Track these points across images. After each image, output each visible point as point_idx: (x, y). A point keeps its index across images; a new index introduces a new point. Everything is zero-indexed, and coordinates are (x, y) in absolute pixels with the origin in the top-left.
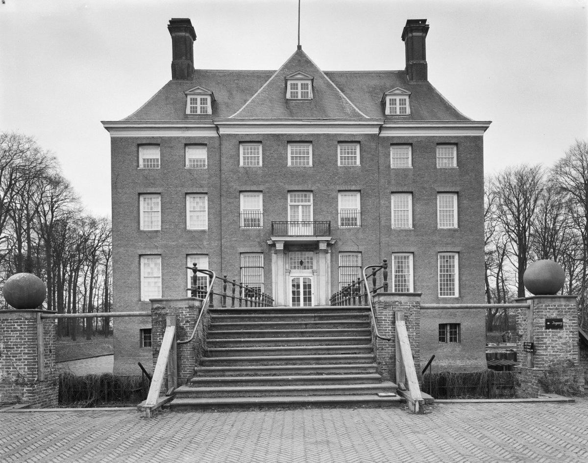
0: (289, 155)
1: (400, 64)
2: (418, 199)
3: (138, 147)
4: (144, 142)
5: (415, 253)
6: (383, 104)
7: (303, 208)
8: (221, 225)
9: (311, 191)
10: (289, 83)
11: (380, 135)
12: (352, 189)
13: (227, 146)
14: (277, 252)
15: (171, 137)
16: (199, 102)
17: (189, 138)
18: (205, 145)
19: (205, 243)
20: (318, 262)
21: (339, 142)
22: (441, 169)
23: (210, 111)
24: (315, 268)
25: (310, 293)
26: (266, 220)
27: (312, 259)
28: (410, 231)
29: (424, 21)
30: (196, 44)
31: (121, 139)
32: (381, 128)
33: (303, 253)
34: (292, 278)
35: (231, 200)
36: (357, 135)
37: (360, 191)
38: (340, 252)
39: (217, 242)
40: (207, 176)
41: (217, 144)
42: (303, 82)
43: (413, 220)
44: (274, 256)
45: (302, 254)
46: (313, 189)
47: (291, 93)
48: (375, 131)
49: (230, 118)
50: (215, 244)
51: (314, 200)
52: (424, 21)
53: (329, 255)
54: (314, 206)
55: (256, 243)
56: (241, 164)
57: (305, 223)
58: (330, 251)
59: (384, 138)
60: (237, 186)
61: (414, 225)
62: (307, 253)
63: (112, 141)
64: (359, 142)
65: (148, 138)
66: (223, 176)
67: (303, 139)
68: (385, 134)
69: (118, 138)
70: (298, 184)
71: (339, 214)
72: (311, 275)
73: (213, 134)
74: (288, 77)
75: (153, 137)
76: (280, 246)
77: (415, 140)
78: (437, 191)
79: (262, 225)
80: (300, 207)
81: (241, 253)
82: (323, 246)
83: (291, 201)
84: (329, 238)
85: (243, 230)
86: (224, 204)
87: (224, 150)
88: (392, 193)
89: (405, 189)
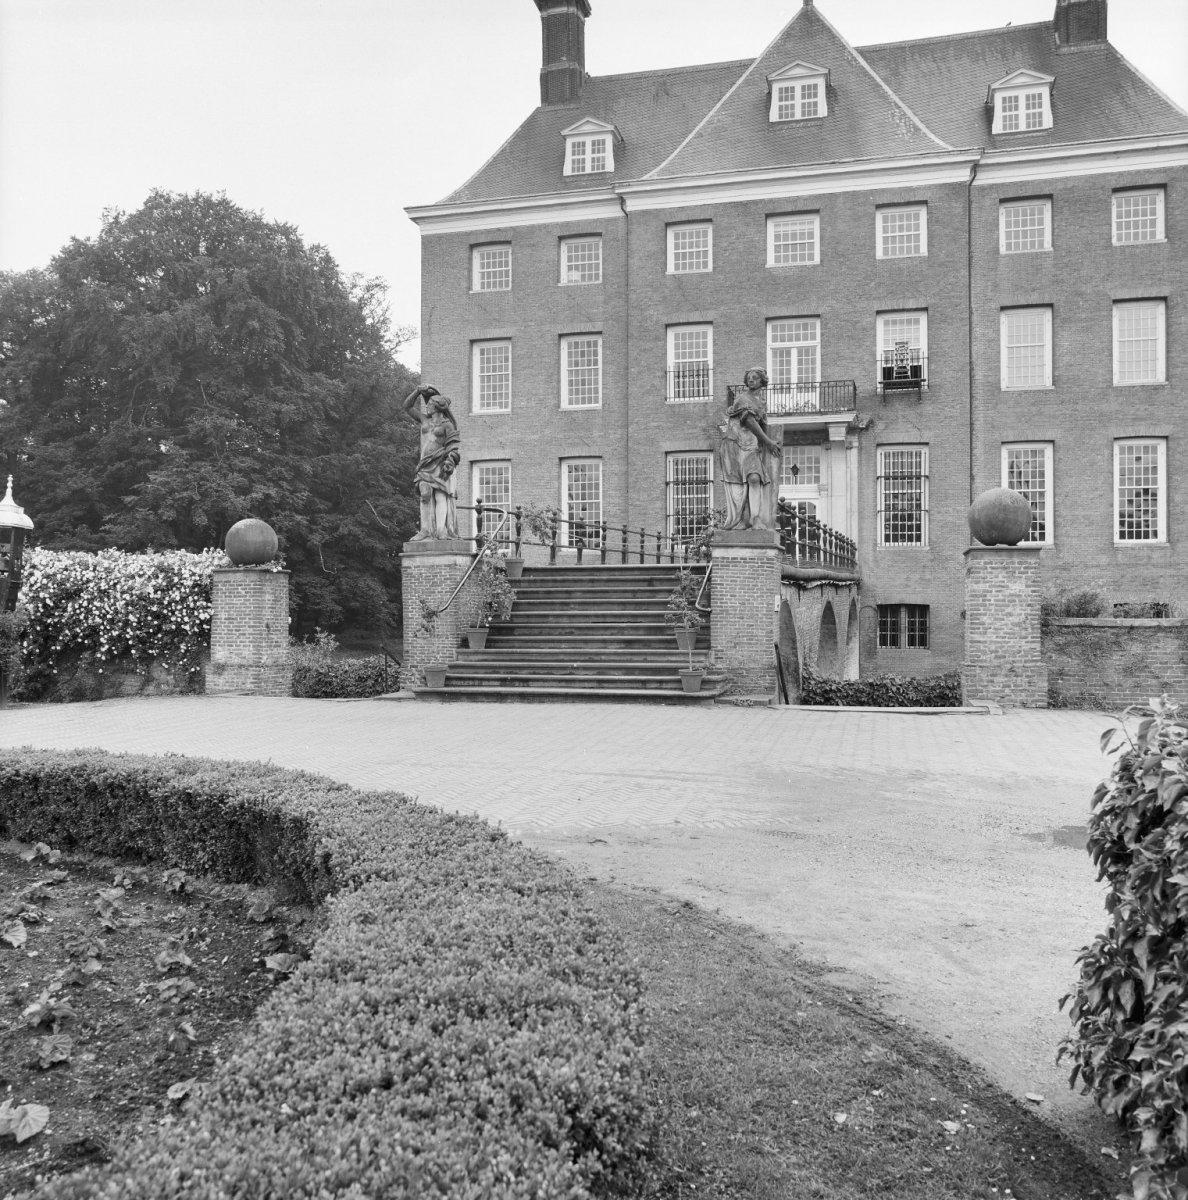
2: (1064, 321)
3: (471, 251)
4: (482, 239)
5: (1057, 441)
6: (988, 113)
7: (800, 353)
8: (626, 397)
9: (818, 316)
10: (776, 87)
11: (974, 183)
13: (642, 241)
15: (533, 226)
16: (589, 148)
17: (567, 224)
18: (599, 235)
19: (596, 434)
20: (829, 467)
21: (879, 207)
22: (1123, 248)
23: (610, 166)
24: (823, 481)
26: (719, 383)
27: (817, 461)
28: (1046, 392)
30: (590, 25)
31: (440, 237)
32: (976, 167)
33: (799, 448)
35: (649, 345)
36: (919, 188)
37: (925, 309)
38: (879, 445)
39: (619, 431)
40: (601, 298)
41: (621, 233)
42: (807, 82)
43: (1054, 368)
45: (795, 453)
47: (781, 108)
48: (963, 175)
49: (644, 178)
50: (615, 435)
51: (822, 335)
53: (854, 452)
56: (671, 269)
57: (805, 386)
58: (856, 444)
59: (982, 188)
60: (657, 314)
62: (807, 448)
63: (423, 243)
64: (925, 202)
65: (488, 232)
66: (633, 296)
67: (800, 207)
68: (984, 179)
69: (434, 236)
71: (879, 363)
72: (815, 495)
73: (613, 212)
74: (773, 76)
75: (499, 230)
77: (1060, 186)
79: (711, 393)
80: (794, 353)
81: (667, 453)
82: (837, 434)
83: (775, 339)
85: (672, 406)
86: (633, 354)
87: (635, 243)
88: (1003, 308)
89: (1034, 299)
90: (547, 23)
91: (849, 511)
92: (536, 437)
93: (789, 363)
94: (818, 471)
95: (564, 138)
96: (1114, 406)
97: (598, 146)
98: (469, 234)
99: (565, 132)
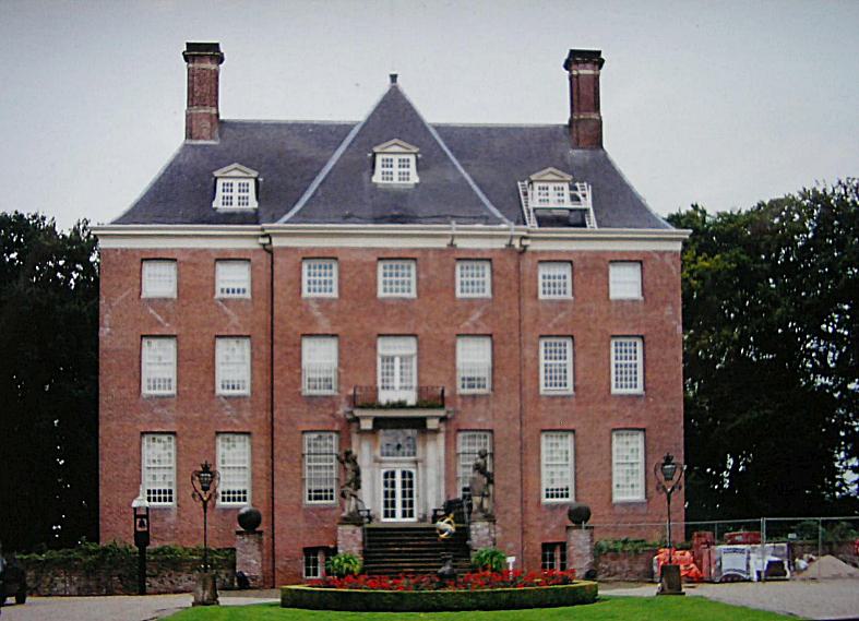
0: (380, 278)
1: (561, 115)
5: (578, 431)
12: (478, 332)
14: (362, 432)
20: (424, 445)
24: (419, 456)
25: (411, 495)
29: (599, 53)
34: (383, 471)
38: (459, 431)
44: (355, 438)
46: (417, 332)
50: (262, 416)
52: (599, 53)
53: (441, 438)
54: (419, 358)
55: (327, 417)
61: (575, 388)
67: (402, 255)
70: (394, 326)
76: (367, 425)
78: (611, 334)
81: (303, 432)
82: (432, 424)
84: (442, 413)
90: (191, 73)
91: (439, 478)
92: (197, 415)
93: (393, 368)
94: (415, 447)
95: (216, 179)
96: (613, 407)
97: (243, 188)
98: (142, 251)
99: (216, 174)
